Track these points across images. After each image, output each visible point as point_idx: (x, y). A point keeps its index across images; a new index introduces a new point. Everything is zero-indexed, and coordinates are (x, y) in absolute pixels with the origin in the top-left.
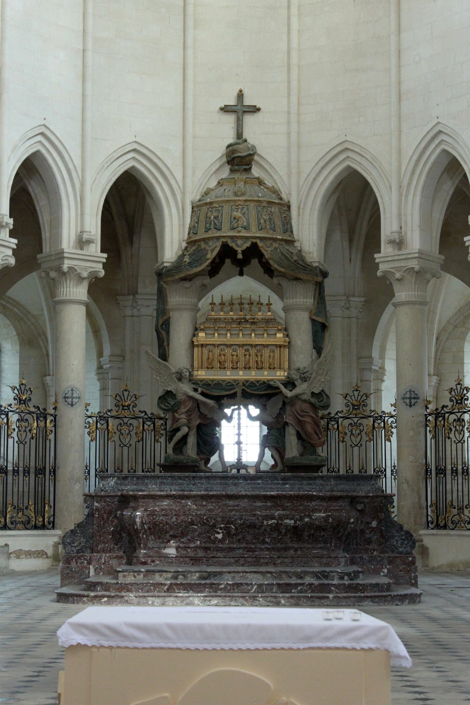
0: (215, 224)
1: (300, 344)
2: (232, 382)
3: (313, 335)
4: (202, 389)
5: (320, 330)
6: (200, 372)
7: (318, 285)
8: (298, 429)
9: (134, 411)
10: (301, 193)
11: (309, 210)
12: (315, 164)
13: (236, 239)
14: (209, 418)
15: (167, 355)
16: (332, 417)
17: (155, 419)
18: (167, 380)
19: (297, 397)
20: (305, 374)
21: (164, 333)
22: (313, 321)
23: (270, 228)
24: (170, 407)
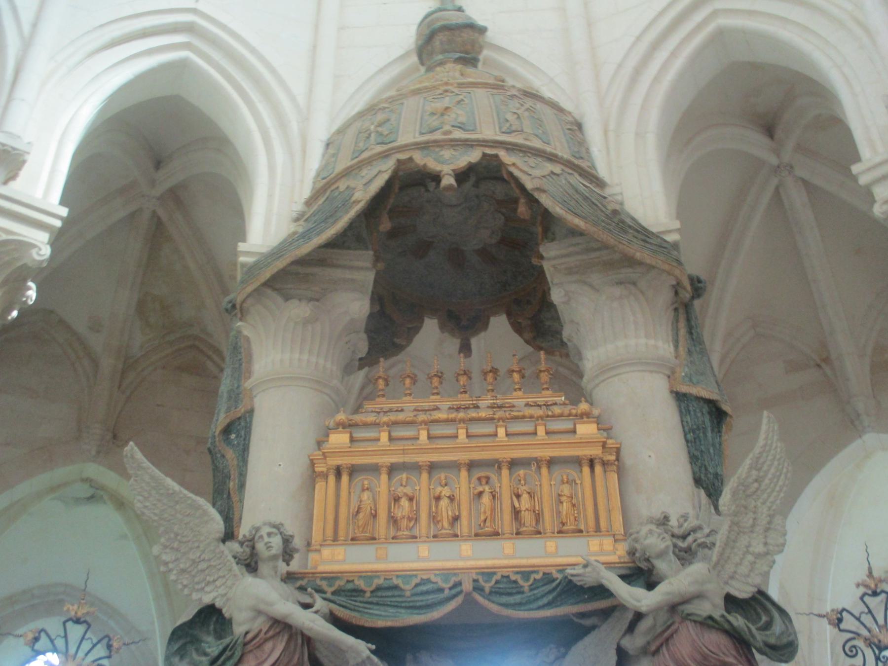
2: (438, 579)
3: (687, 441)
4: (333, 606)
5: (708, 423)
6: (326, 552)
13: (437, 149)
15: (236, 517)
20: (690, 539)
22: (680, 397)
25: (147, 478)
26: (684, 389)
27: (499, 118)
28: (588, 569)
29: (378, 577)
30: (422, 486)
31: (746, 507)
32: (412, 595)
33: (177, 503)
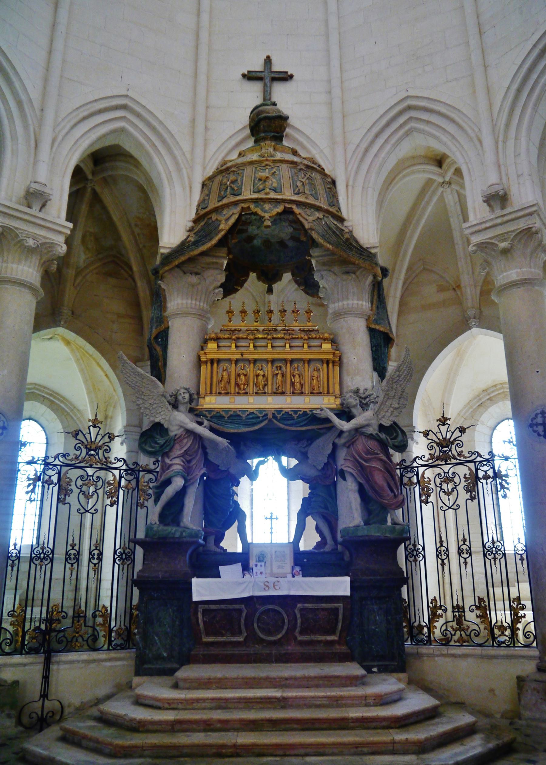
0: (232, 189)
1: (355, 361)
2: (257, 413)
4: (210, 423)
6: (207, 399)
7: (376, 286)
8: (361, 481)
9: (106, 458)
10: (349, 169)
11: (360, 189)
12: (366, 130)
13: (262, 203)
14: (223, 471)
16: (408, 467)
17: (139, 471)
18: (155, 406)
19: (358, 431)
20: (368, 399)
21: (158, 349)
23: (311, 195)
24: (158, 448)
25: (129, 367)
26: (373, 326)
27: (293, 184)
28: (323, 412)
29: (231, 411)
30: (250, 369)
31: (392, 388)
32: (246, 419)
33: (143, 379)
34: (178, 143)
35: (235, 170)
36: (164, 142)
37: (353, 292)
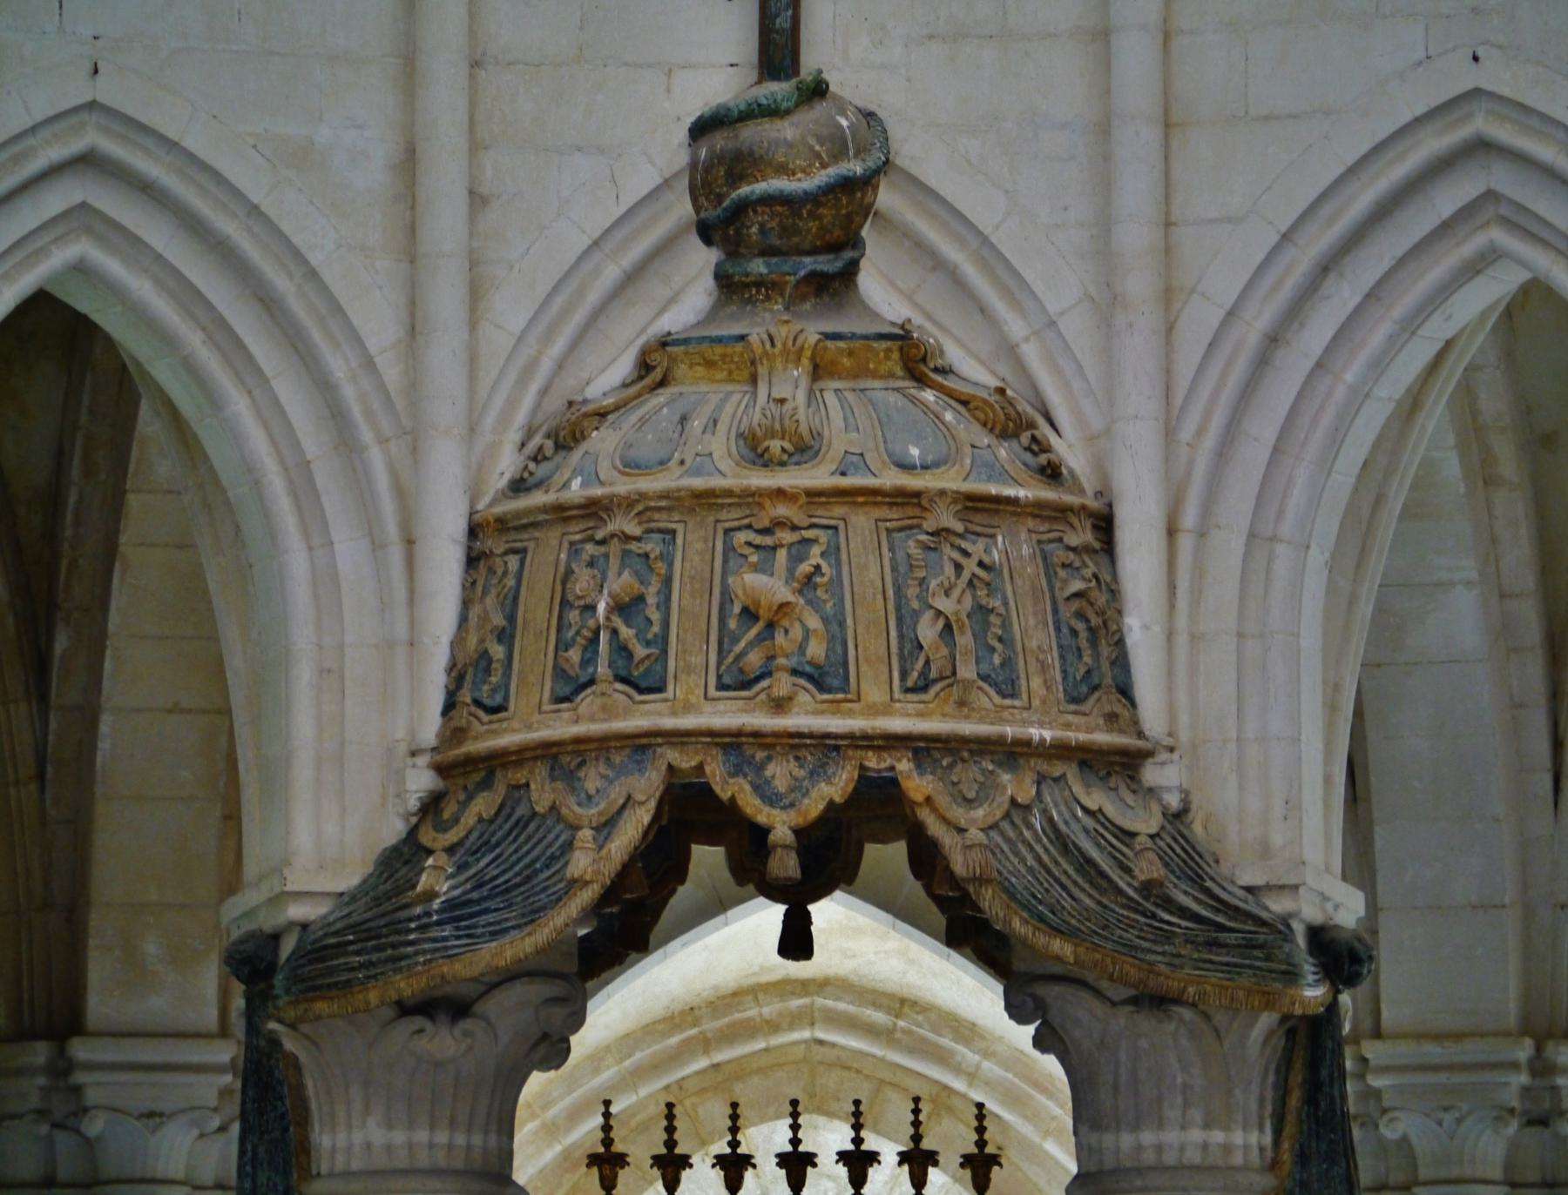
10: (1186, 433)
11: (1237, 544)
12: (1274, 238)
13: (760, 755)
27: (901, 636)
34: (338, 310)
35: (633, 529)
36: (267, 302)
37: (1186, 1087)
